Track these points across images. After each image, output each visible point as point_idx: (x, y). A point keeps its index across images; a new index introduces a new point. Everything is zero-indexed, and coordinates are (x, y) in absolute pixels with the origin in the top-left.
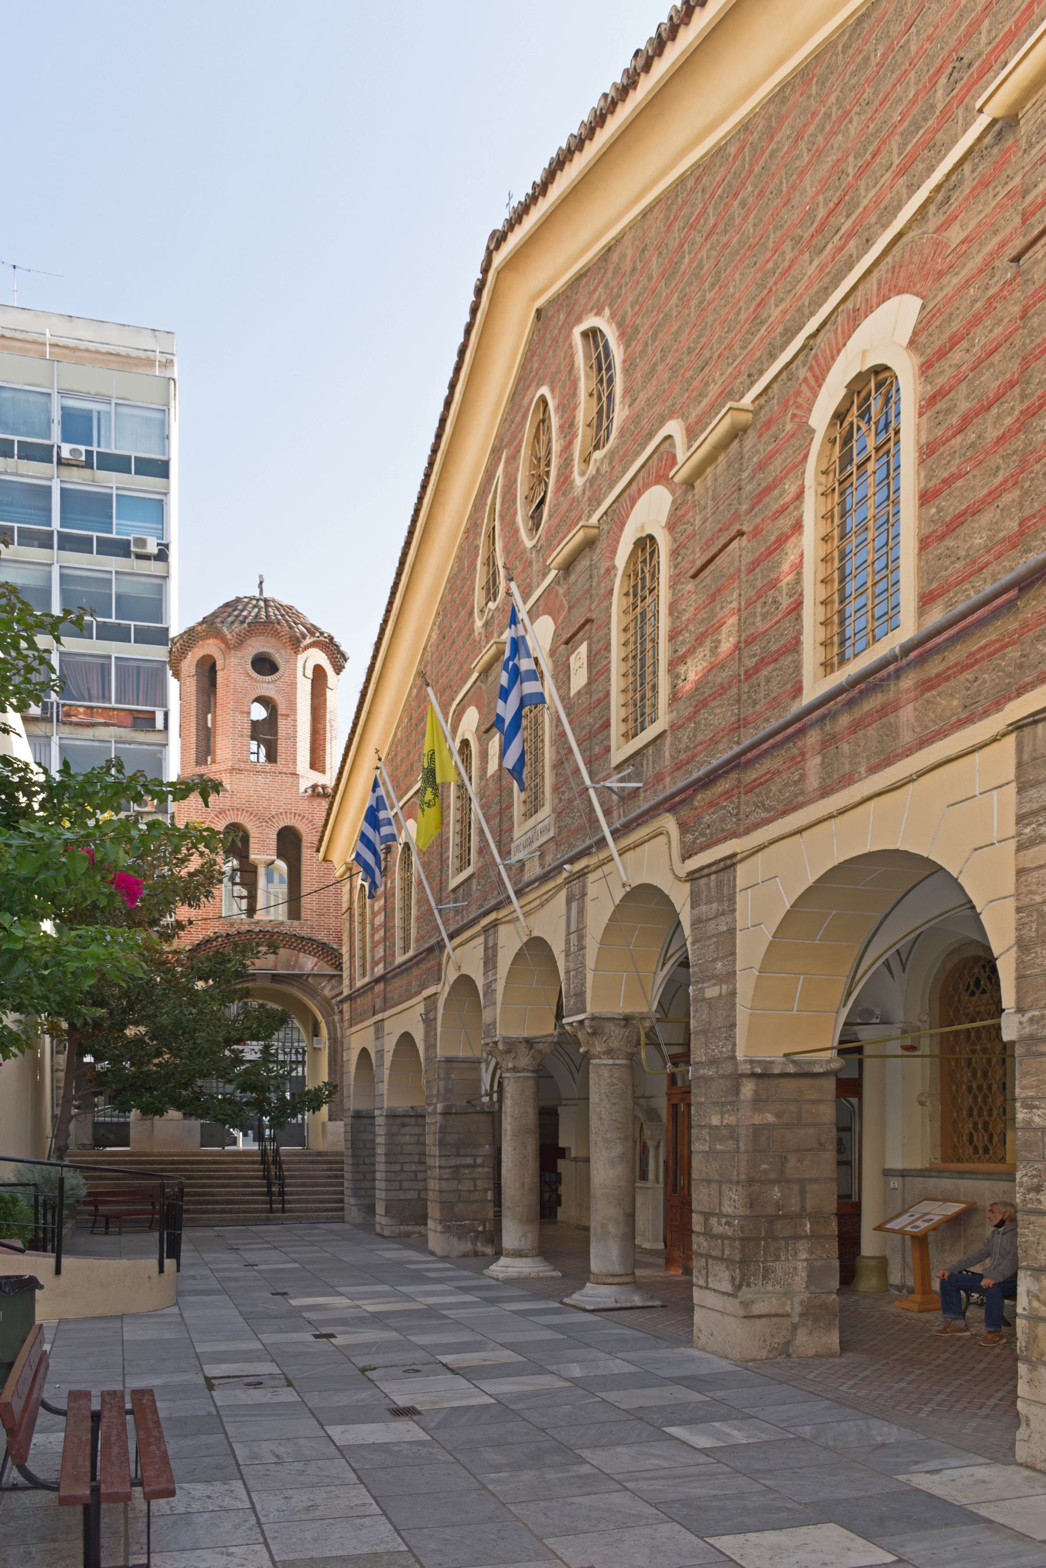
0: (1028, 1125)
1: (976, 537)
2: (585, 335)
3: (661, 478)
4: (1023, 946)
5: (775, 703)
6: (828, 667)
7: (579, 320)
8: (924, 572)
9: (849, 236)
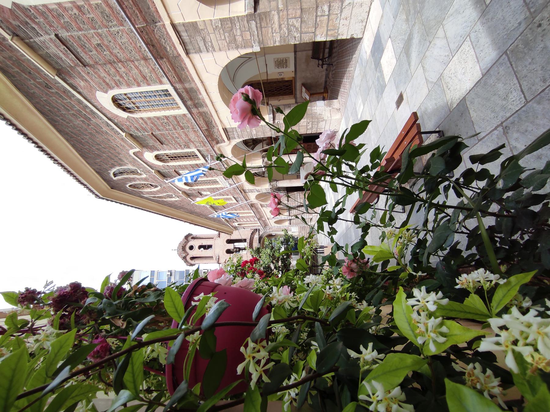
0: (280, 41)
1: (146, 71)
2: (115, 177)
3: (142, 154)
4: (237, 48)
5: (188, 121)
6: (179, 108)
7: (112, 178)
8: (155, 83)
9: (86, 112)
